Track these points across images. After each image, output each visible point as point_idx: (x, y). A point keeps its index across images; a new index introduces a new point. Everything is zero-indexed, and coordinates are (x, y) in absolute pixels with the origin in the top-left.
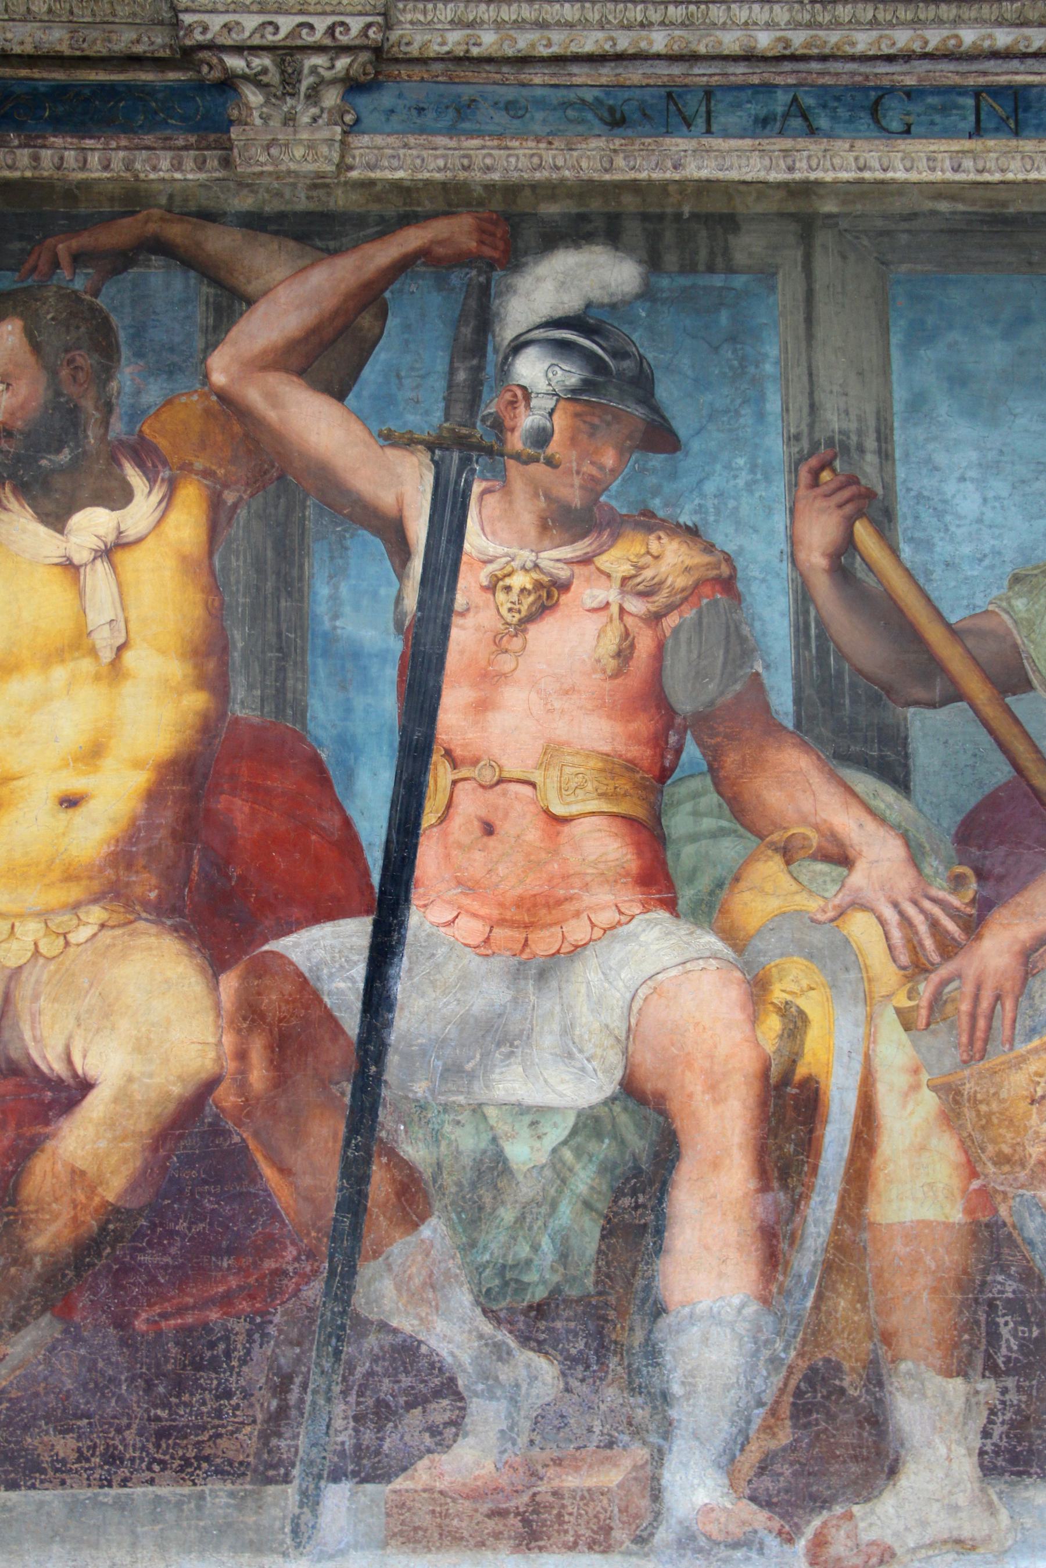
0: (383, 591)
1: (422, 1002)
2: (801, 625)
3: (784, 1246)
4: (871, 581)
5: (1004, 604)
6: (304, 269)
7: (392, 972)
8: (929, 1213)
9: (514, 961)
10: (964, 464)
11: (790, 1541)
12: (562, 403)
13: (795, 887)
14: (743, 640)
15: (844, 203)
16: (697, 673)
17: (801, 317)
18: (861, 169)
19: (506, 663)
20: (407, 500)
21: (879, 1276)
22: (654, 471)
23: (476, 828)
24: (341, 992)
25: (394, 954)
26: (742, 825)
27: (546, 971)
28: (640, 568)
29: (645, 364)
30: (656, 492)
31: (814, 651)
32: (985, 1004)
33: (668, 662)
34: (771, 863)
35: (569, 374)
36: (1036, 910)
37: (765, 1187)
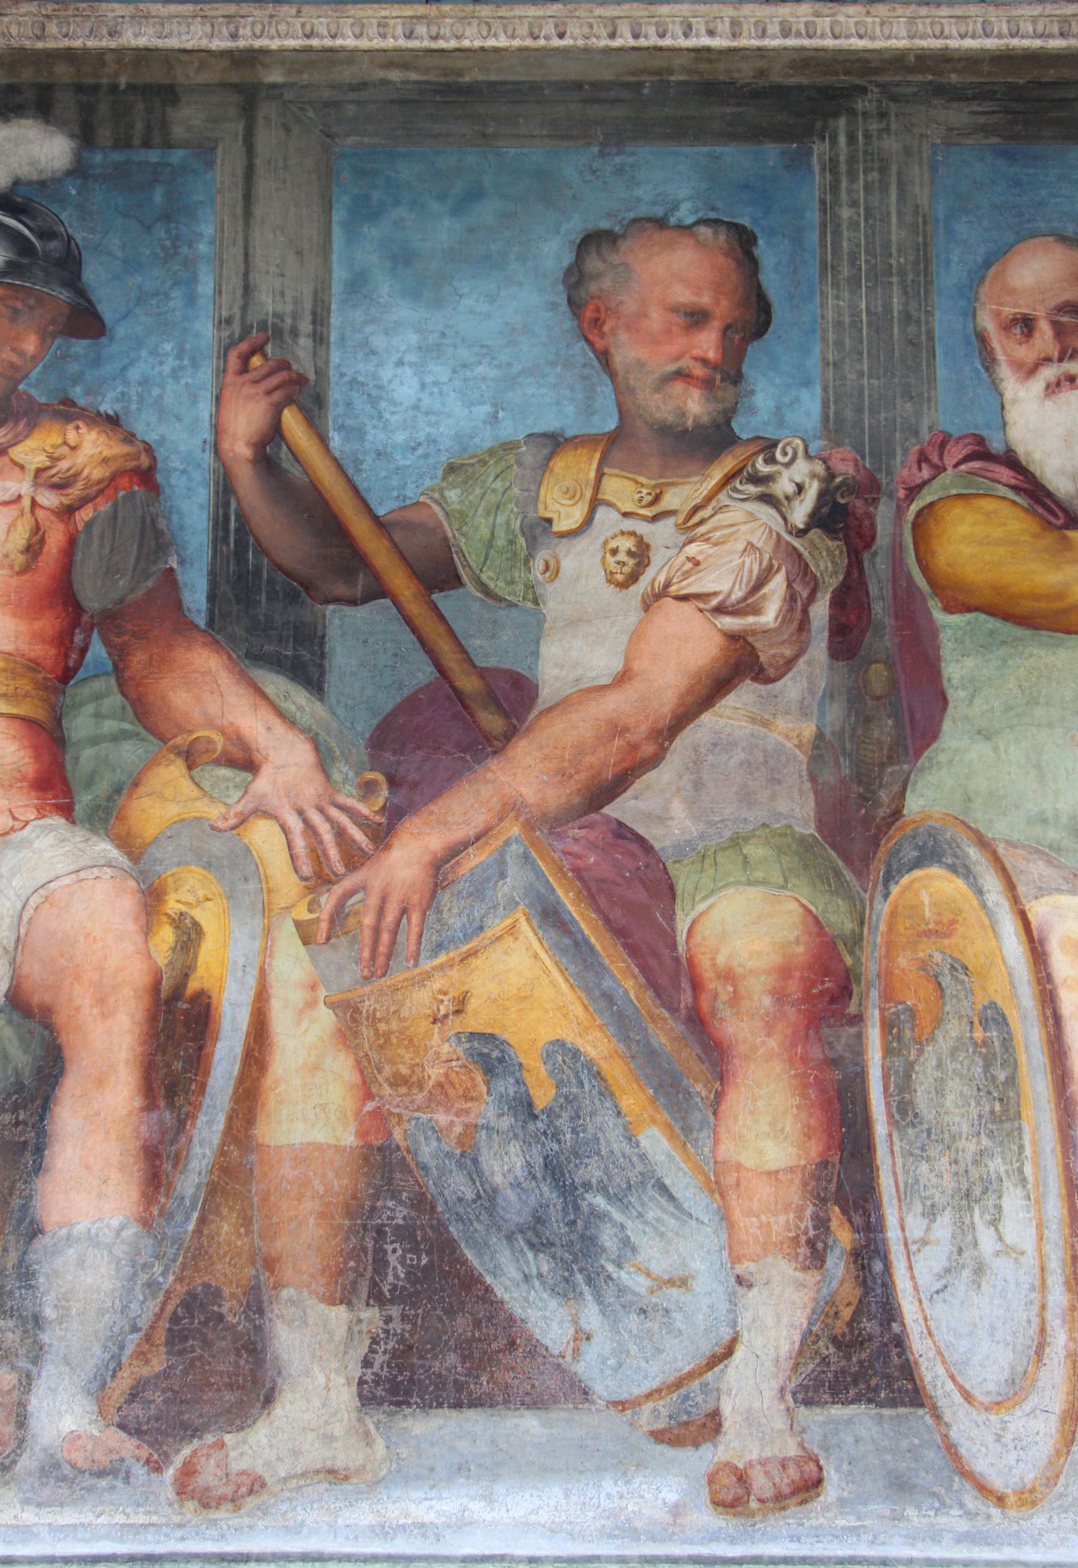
2: (221, 519)
3: (168, 1166)
4: (295, 471)
5: (437, 495)
8: (319, 1135)
10: (403, 348)
11: (158, 1469)
13: (196, 793)
14: (158, 534)
15: (290, 72)
16: (108, 568)
17: (239, 194)
18: (308, 36)
21: (265, 1199)
22: (77, 358)
26: (145, 727)
28: (55, 460)
29: (73, 245)
31: (232, 545)
32: (390, 918)
33: (78, 557)
34: (172, 768)
36: (450, 819)
37: (150, 1105)
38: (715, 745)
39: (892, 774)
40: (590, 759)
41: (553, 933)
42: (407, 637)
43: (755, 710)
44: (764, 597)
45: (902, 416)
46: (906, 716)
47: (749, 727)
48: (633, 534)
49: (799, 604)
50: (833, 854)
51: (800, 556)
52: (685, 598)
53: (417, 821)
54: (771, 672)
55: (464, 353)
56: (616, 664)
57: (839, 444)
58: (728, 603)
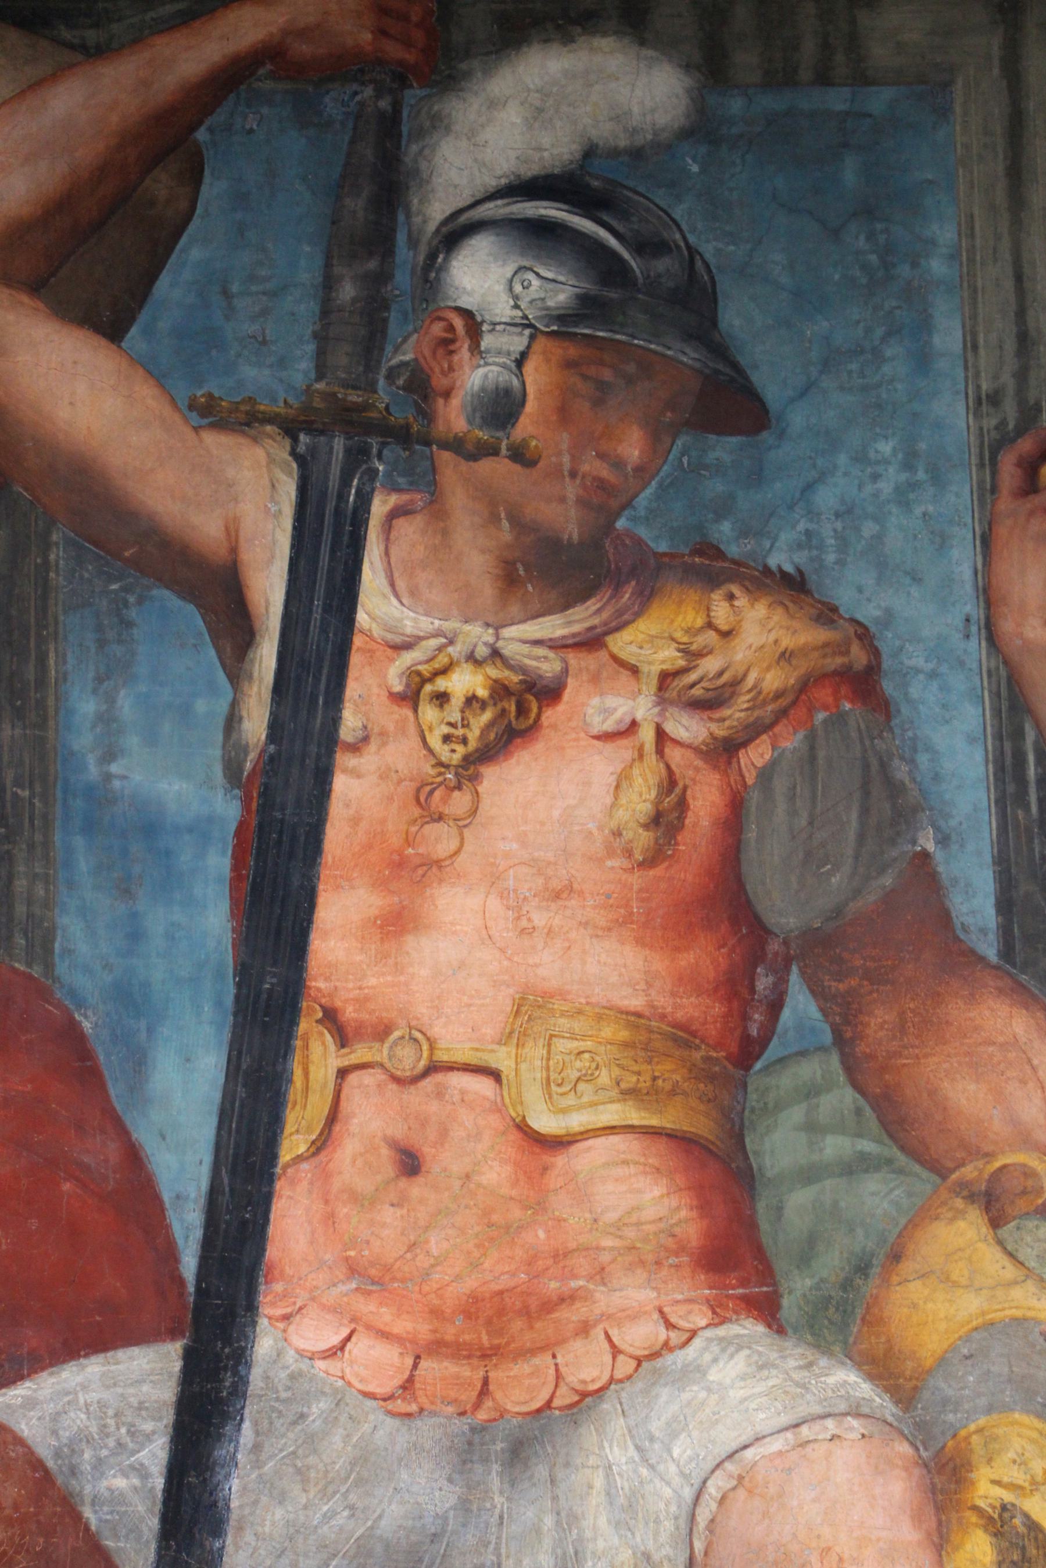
0: (201, 706)
1: (279, 1513)
2: (1009, 760)
6: (35, 86)
7: (221, 1452)
9: (461, 1425)
12: (541, 343)
13: (1010, 1271)
14: (895, 789)
16: (808, 854)
19: (440, 840)
20: (247, 528)
23: (386, 1161)
24: (117, 1498)
25: (225, 1417)
26: (902, 1148)
27: (523, 1445)
28: (693, 655)
29: (699, 264)
30: (723, 508)
31: (1034, 809)
33: (751, 834)
34: (962, 1224)
35: (553, 286)
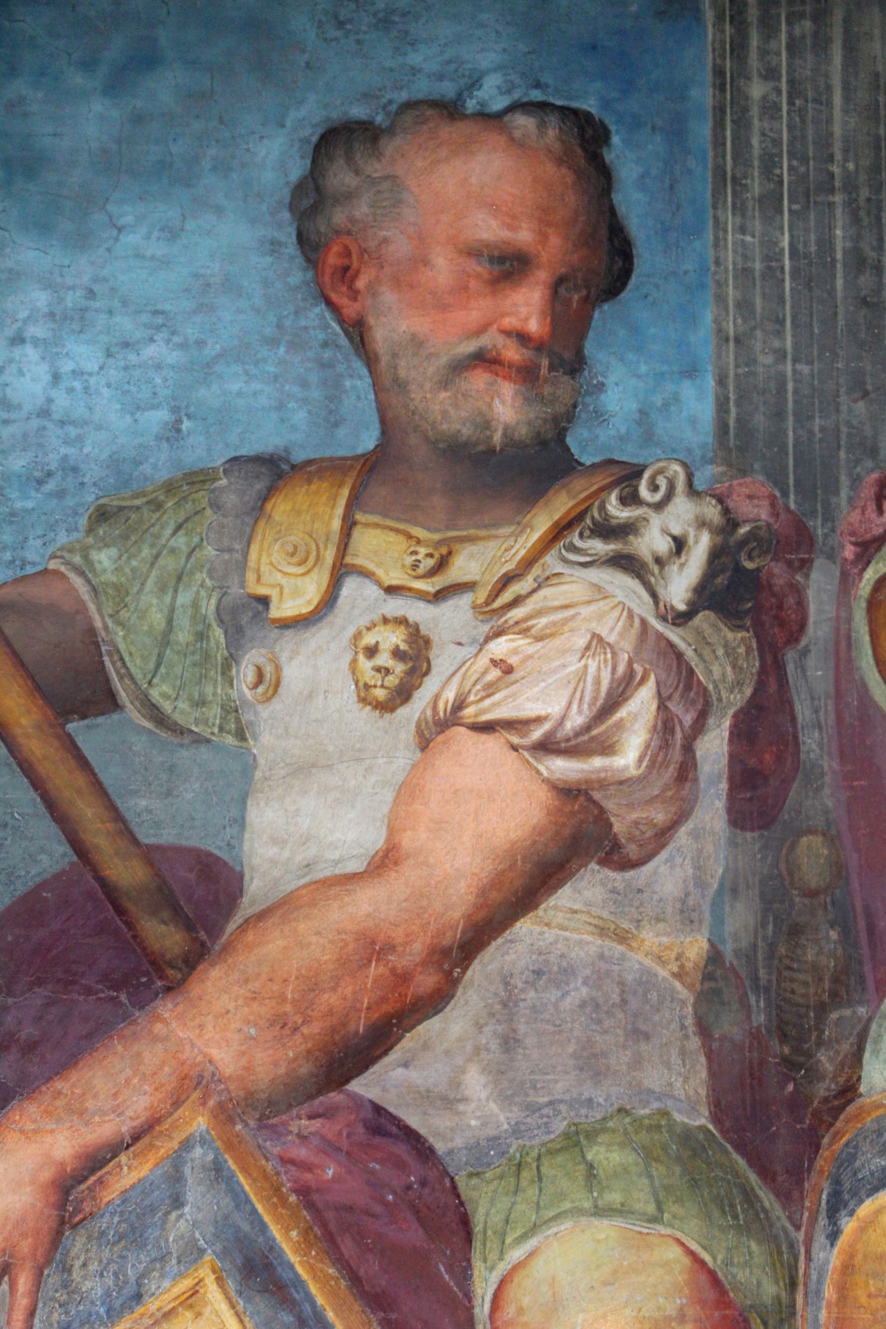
5: (77, 559)
10: (23, 314)
36: (90, 1104)
38: (538, 973)
39: (839, 1021)
40: (329, 999)
41: (261, 1303)
42: (23, 795)
43: (605, 914)
44: (620, 726)
45: (849, 424)
46: (862, 924)
47: (595, 944)
48: (402, 621)
49: (679, 735)
50: (741, 1162)
51: (679, 655)
52: (488, 728)
53: (33, 1108)
54: (632, 851)
55: (125, 324)
56: (374, 839)
57: (743, 472)
58: (559, 735)
